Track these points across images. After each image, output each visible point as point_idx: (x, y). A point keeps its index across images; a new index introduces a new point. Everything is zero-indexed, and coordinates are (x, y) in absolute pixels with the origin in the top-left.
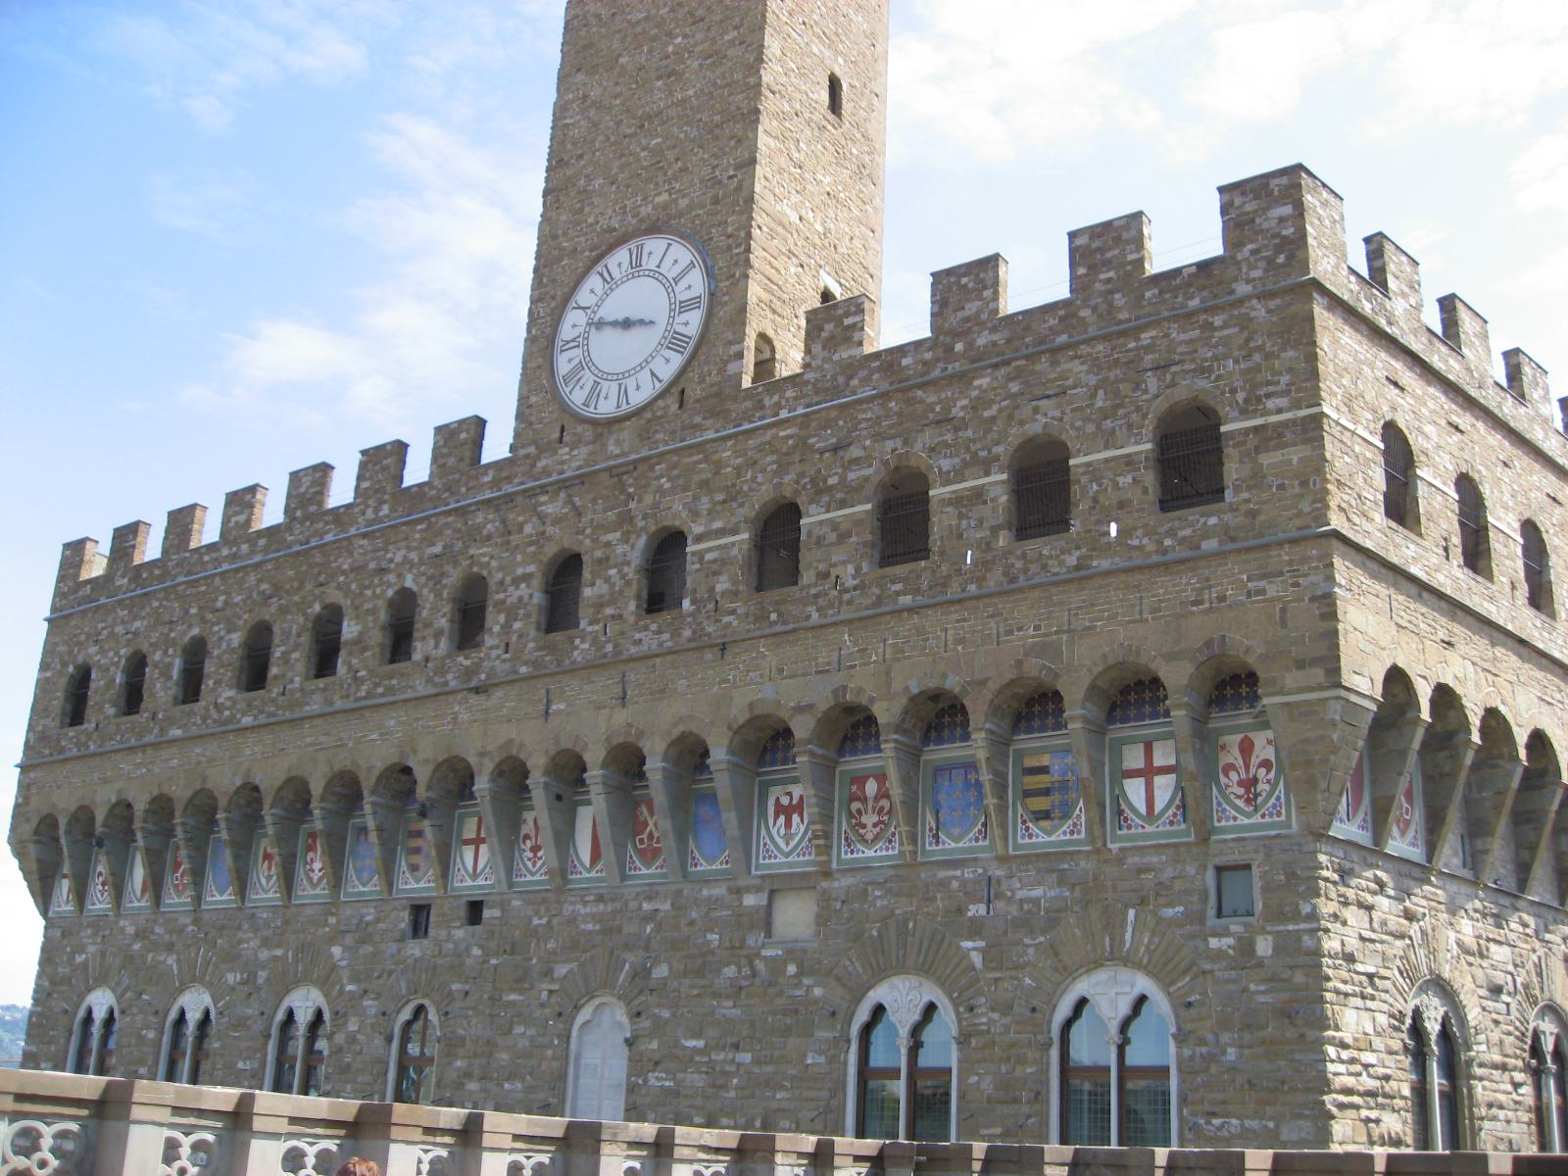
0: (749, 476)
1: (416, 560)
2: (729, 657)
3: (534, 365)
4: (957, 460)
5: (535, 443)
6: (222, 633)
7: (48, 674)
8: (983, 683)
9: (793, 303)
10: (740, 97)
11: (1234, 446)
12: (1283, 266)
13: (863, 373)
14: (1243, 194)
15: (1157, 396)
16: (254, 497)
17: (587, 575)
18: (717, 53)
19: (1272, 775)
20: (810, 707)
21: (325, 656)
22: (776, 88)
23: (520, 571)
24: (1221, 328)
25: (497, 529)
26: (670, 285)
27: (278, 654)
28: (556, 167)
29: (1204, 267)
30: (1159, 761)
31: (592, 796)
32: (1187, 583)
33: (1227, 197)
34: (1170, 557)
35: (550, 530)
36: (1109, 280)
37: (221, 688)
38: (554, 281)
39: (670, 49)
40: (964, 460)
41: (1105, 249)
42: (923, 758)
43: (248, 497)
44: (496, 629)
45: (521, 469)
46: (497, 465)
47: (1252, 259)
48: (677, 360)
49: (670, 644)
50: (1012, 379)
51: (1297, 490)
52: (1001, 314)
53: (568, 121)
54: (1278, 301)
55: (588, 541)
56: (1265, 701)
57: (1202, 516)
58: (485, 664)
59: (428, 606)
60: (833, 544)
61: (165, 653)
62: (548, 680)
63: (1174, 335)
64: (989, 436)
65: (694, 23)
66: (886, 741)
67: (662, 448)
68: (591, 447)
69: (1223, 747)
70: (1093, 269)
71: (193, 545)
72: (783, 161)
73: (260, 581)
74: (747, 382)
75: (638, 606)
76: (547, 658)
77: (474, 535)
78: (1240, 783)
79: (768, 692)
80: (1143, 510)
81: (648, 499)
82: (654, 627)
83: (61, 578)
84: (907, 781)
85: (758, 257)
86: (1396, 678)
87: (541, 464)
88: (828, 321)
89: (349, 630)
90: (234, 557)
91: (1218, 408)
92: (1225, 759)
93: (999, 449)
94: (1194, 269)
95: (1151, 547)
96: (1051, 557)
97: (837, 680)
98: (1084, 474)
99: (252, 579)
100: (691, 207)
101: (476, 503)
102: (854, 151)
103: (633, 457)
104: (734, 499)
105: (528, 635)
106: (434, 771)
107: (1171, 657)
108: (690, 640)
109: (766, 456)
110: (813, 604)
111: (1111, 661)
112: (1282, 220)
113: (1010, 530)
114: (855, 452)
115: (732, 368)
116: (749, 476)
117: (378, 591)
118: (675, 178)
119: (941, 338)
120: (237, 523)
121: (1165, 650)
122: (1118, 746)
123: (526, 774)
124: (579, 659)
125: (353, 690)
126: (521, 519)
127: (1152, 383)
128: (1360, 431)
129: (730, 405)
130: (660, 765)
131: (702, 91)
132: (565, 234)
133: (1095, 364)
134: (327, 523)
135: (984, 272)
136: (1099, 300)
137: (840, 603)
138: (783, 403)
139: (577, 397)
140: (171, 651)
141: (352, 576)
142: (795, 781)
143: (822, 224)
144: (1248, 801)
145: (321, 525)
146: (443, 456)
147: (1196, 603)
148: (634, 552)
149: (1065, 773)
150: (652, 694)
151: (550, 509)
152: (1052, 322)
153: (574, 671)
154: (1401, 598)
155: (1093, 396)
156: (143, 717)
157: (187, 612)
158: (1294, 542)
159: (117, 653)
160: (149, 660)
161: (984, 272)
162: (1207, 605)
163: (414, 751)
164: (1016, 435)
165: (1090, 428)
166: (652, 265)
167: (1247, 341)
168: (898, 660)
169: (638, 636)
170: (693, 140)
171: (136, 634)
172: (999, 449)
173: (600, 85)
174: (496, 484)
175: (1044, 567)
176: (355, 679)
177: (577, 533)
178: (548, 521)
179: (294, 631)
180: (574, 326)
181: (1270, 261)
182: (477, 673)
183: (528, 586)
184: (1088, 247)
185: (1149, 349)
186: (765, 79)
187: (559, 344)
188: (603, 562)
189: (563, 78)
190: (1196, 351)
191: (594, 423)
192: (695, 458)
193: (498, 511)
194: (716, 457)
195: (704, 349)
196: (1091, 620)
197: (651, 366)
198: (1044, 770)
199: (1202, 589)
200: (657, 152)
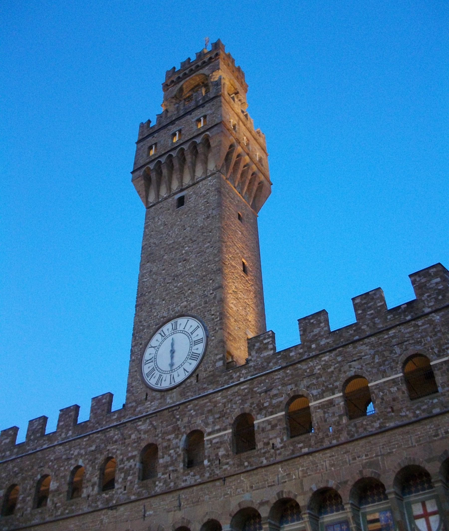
0: (229, 406)
1: (84, 453)
2: (227, 483)
3: (134, 370)
4: (319, 390)
5: (135, 401)
8: (346, 482)
11: (438, 370)
12: (442, 299)
14: (420, 276)
17: (160, 453)
18: (202, 251)
20: (267, 502)
23: (130, 455)
24: (421, 326)
25: (119, 438)
26: (189, 335)
27: (20, 498)
28: (139, 297)
29: (410, 304)
30: (429, 510)
32: (429, 428)
33: (413, 278)
34: (420, 417)
35: (143, 436)
36: (372, 314)
38: (141, 338)
39: (184, 252)
41: (368, 303)
44: (120, 480)
45: (130, 412)
47: (428, 299)
48: (194, 364)
49: (199, 480)
50: (338, 356)
55: (160, 439)
57: (430, 399)
58: (115, 496)
59: (89, 472)
60: (269, 430)
62: (144, 501)
63: (403, 331)
64: (332, 379)
65: (192, 242)
66: (305, 514)
67: (191, 398)
68: (160, 401)
70: (364, 310)
73: (14, 467)
75: (184, 465)
76: (144, 491)
77: (109, 441)
79: (247, 497)
80: (404, 400)
81: (186, 420)
82: (192, 473)
88: (256, 342)
89: (53, 485)
93: (337, 384)
94: (405, 306)
95: (411, 415)
96: (367, 425)
97: (277, 489)
98: (375, 389)
99: (10, 466)
100: (196, 306)
103: (178, 403)
104: (224, 416)
105: (134, 482)
107: (429, 460)
108: (208, 478)
109: (236, 397)
110: (263, 457)
111: (403, 466)
112: (437, 283)
113: (347, 415)
114: (274, 392)
116: (229, 406)
118: (189, 296)
120: (5, 443)
121: (426, 458)
124: (159, 491)
125: (54, 512)
126: (130, 432)
127: (397, 350)
129: (218, 379)
131: (197, 265)
132: (145, 320)
133: (372, 346)
134: (44, 441)
135: (321, 316)
136: (369, 322)
137: (276, 455)
138: (241, 375)
139: (152, 382)
141: (55, 462)
145: (42, 441)
146: (95, 409)
148: (181, 441)
149: (387, 521)
150: (193, 503)
151: (143, 427)
152: (351, 332)
155: (374, 358)
161: (321, 316)
165: (374, 371)
166: (182, 328)
168: (305, 477)
169: (184, 478)
170: (195, 282)
172: (337, 384)
173: (156, 266)
174: (118, 419)
175: (365, 429)
176: (55, 507)
177: (155, 436)
178: (142, 433)
179: (28, 488)
180: (150, 354)
181: (436, 299)
182: (112, 500)
183: (134, 460)
184: (360, 303)
185: (393, 337)
187: (144, 361)
188: (167, 448)
189: (142, 266)
190: (413, 335)
192: (206, 401)
193: (120, 430)
194: (214, 400)
195: (205, 358)
196: (390, 449)
198: (377, 521)
200: (180, 288)
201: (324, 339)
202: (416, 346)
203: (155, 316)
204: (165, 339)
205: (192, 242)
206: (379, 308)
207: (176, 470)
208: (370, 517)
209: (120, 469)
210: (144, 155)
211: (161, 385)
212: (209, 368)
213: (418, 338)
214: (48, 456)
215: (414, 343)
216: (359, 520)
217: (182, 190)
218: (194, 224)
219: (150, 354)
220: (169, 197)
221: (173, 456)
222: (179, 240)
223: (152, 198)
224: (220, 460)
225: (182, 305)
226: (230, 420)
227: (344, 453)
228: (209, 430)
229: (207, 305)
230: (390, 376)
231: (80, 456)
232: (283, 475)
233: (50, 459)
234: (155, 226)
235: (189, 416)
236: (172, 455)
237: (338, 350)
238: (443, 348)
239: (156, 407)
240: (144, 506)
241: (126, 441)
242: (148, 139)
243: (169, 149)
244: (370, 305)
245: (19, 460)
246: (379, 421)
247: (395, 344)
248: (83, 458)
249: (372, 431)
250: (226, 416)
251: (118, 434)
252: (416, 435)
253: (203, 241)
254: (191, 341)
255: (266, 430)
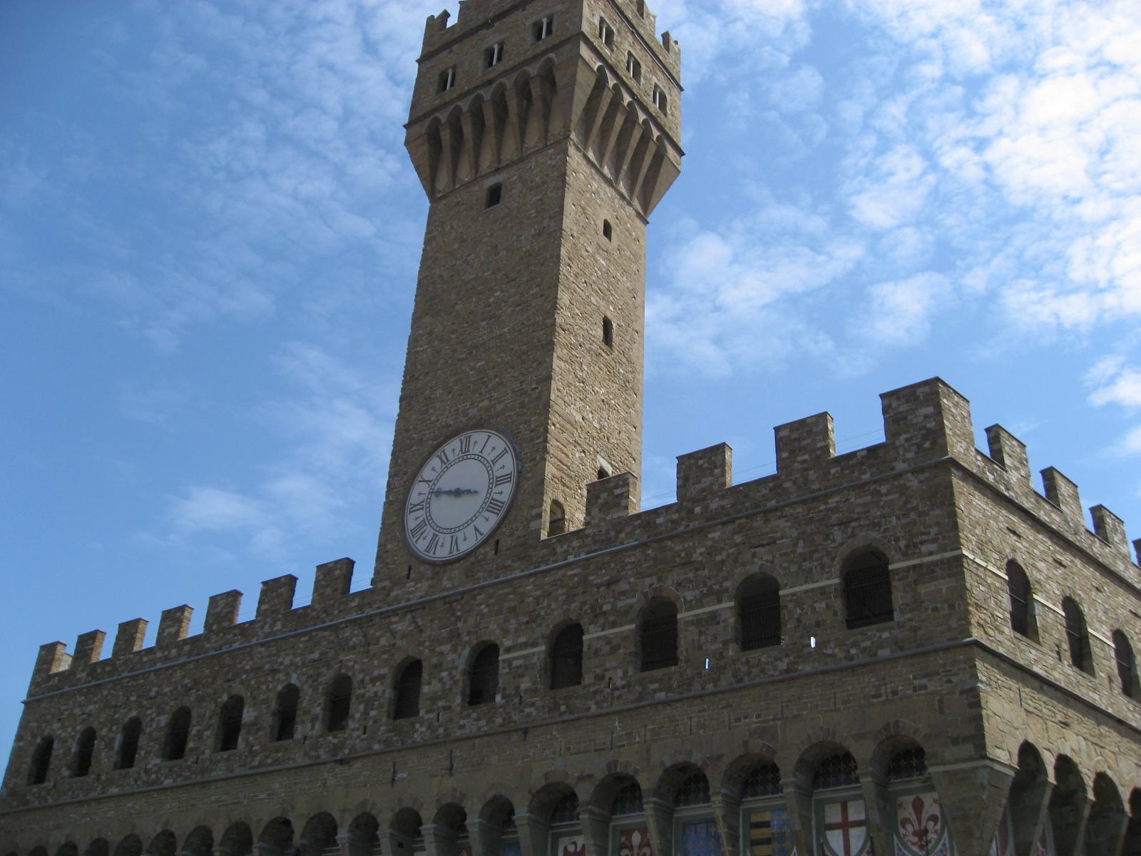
1: (300, 664)
3: (390, 522)
4: (697, 592)
6: (154, 716)
7: (21, 744)
8: (719, 758)
9: (577, 478)
10: (541, 333)
11: (899, 580)
13: (628, 529)
14: (898, 399)
15: (841, 544)
16: (183, 614)
17: (425, 676)
19: (938, 827)
20: (590, 777)
21: (229, 734)
22: (566, 327)
23: (376, 673)
24: (887, 494)
26: (489, 465)
27: (194, 732)
29: (872, 450)
30: (852, 816)
31: (426, 844)
33: (887, 401)
34: (855, 662)
35: (399, 643)
36: (804, 461)
37: (150, 758)
38: (406, 461)
39: (492, 300)
40: (702, 592)
41: (801, 440)
42: (675, 815)
43: (178, 614)
44: (358, 716)
46: (362, 594)
48: (494, 519)
49: (485, 728)
50: (735, 533)
51: (946, 612)
52: (728, 486)
53: (419, 349)
54: (927, 475)
55: (427, 651)
56: (931, 770)
57: (878, 631)
59: (307, 698)
61: (110, 730)
63: (852, 500)
65: (508, 282)
66: (647, 803)
67: (482, 583)
68: (430, 582)
69: (901, 806)
70: (793, 453)
71: (136, 649)
72: (571, 378)
73: (184, 677)
74: (544, 535)
75: (463, 700)
76: (395, 739)
78: (915, 834)
81: (471, 620)
82: (474, 715)
83: (37, 672)
84: (663, 833)
85: (552, 446)
86: (1028, 751)
87: (393, 594)
89: (248, 715)
90: (166, 659)
91: (886, 552)
92: (902, 815)
93: (728, 584)
94: (865, 453)
95: (841, 655)
96: (767, 663)
98: (791, 601)
99: (178, 675)
101: (346, 622)
102: (621, 371)
103: (460, 589)
104: (534, 621)
106: (308, 823)
112: (926, 417)
113: (737, 643)
114: (623, 586)
115: (533, 525)
117: (271, 686)
119: (685, 503)
122: (820, 806)
123: (376, 826)
124: (419, 739)
125: (249, 759)
126: (378, 634)
127: (838, 534)
128: (990, 568)
130: (477, 820)
134: (235, 635)
137: (612, 698)
138: (571, 551)
139: (421, 545)
140: (114, 728)
141: (252, 674)
142: (579, 833)
143: (599, 423)
144: (921, 847)
145: (231, 636)
147: (875, 696)
148: (460, 659)
152: (764, 491)
153: (413, 748)
154: (1027, 690)
155: (795, 545)
156: (90, 778)
157: (128, 699)
158: (946, 649)
159: (74, 729)
160: (97, 734)
162: (884, 698)
163: (293, 808)
164: (740, 573)
165: (794, 568)
166: (477, 451)
167: (905, 503)
169: (462, 722)
171: (89, 715)
172: (728, 584)
174: (360, 608)
175: (763, 671)
176: (251, 752)
177: (419, 645)
179: (207, 715)
180: (420, 494)
181: (919, 446)
183: (382, 684)
186: (558, 321)
187: (409, 507)
188: (438, 667)
190: (869, 511)
191: (433, 564)
194: (521, 590)
197: (475, 523)
198: (766, 824)
199: (880, 686)
201: (717, 499)
202: (869, 532)
203: (434, 422)
204: (447, 468)
205: (508, 282)
206: (818, 452)
207: (450, 708)
208: (755, 818)
209: (358, 697)
210: (431, 89)
211: (434, 554)
212: (517, 530)
213: (877, 518)
214: (240, 663)
215: (868, 525)
216: (738, 820)
217: (498, 170)
218: (515, 243)
219: (420, 494)
220: (475, 181)
221: (445, 684)
222: (486, 274)
223: (443, 182)
224: (521, 697)
225: (481, 404)
226: (545, 629)
227: (723, 708)
228: (507, 643)
229: (525, 411)
230: (817, 581)
231: (293, 668)
232: (621, 734)
233: (243, 668)
234: (444, 241)
235: (477, 615)
236: (444, 680)
237: (738, 522)
238: (915, 541)
239: (423, 593)
240: (394, 764)
241: (371, 648)
242: (441, 55)
243: (479, 82)
244: (804, 443)
245: (191, 666)
246: (787, 660)
247: (836, 523)
248: (299, 672)
249: (772, 676)
250: (539, 622)
251: (357, 635)
252: (844, 691)
253: (528, 281)
254: (491, 476)
255: (602, 653)
